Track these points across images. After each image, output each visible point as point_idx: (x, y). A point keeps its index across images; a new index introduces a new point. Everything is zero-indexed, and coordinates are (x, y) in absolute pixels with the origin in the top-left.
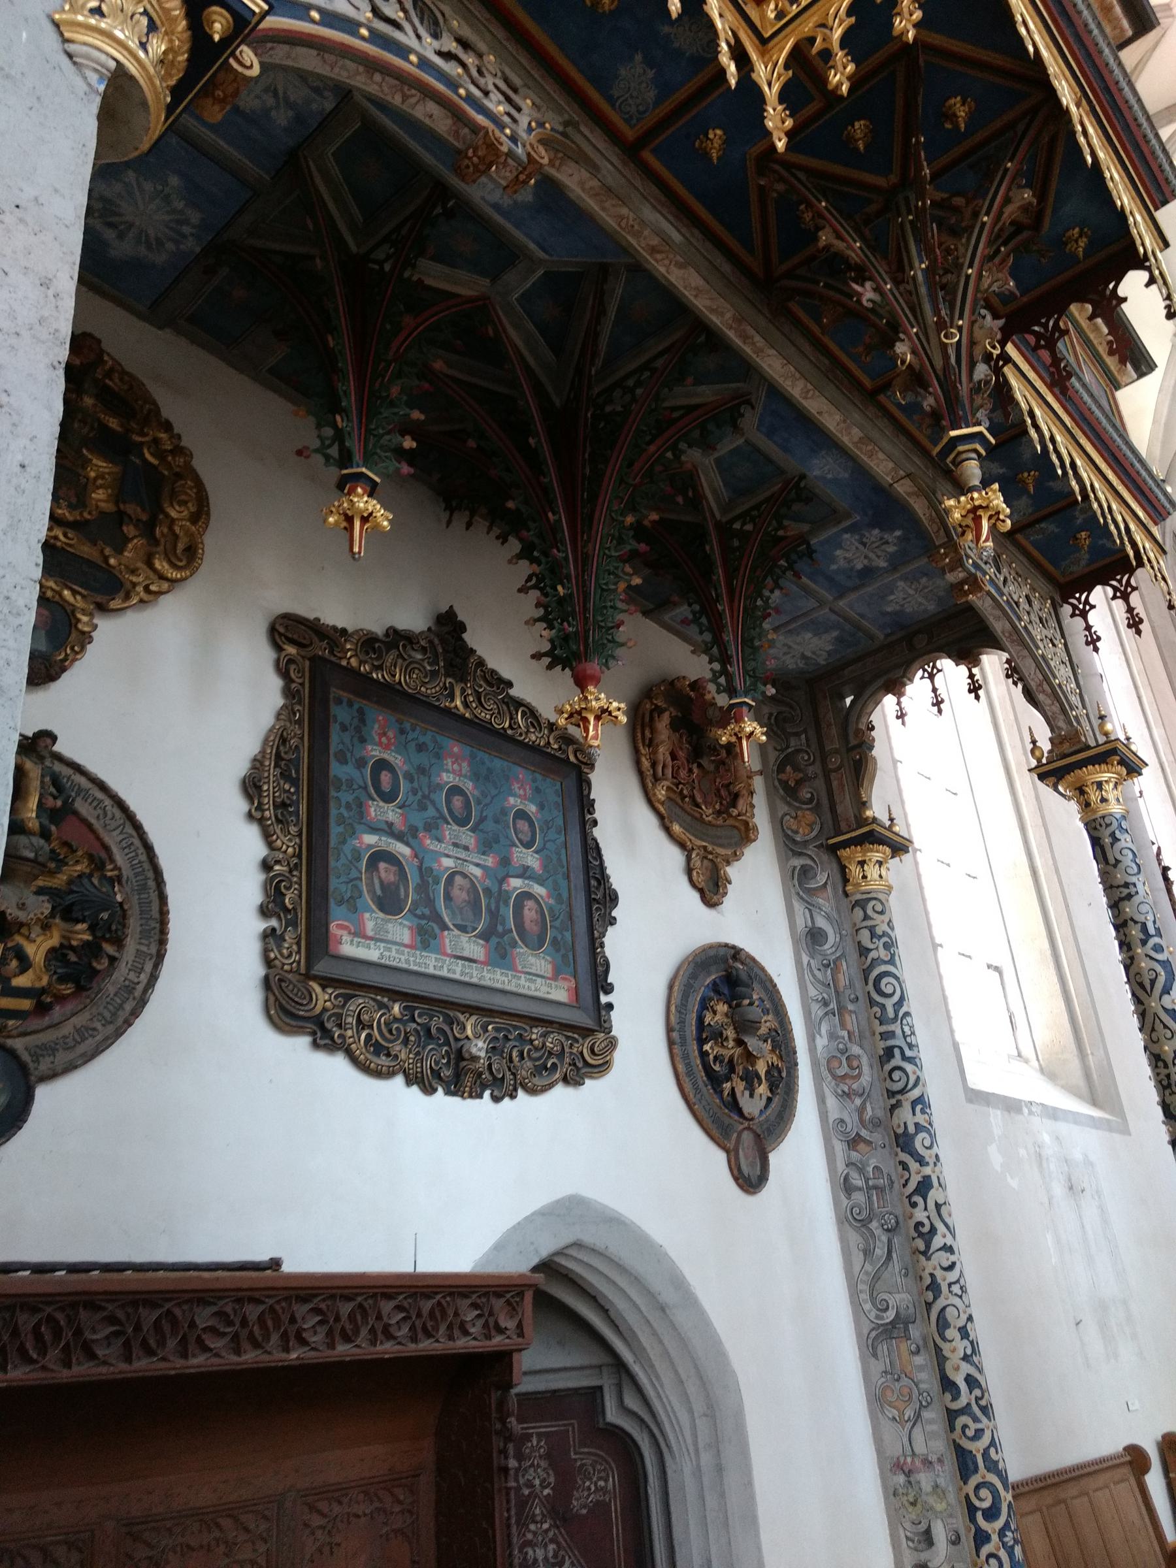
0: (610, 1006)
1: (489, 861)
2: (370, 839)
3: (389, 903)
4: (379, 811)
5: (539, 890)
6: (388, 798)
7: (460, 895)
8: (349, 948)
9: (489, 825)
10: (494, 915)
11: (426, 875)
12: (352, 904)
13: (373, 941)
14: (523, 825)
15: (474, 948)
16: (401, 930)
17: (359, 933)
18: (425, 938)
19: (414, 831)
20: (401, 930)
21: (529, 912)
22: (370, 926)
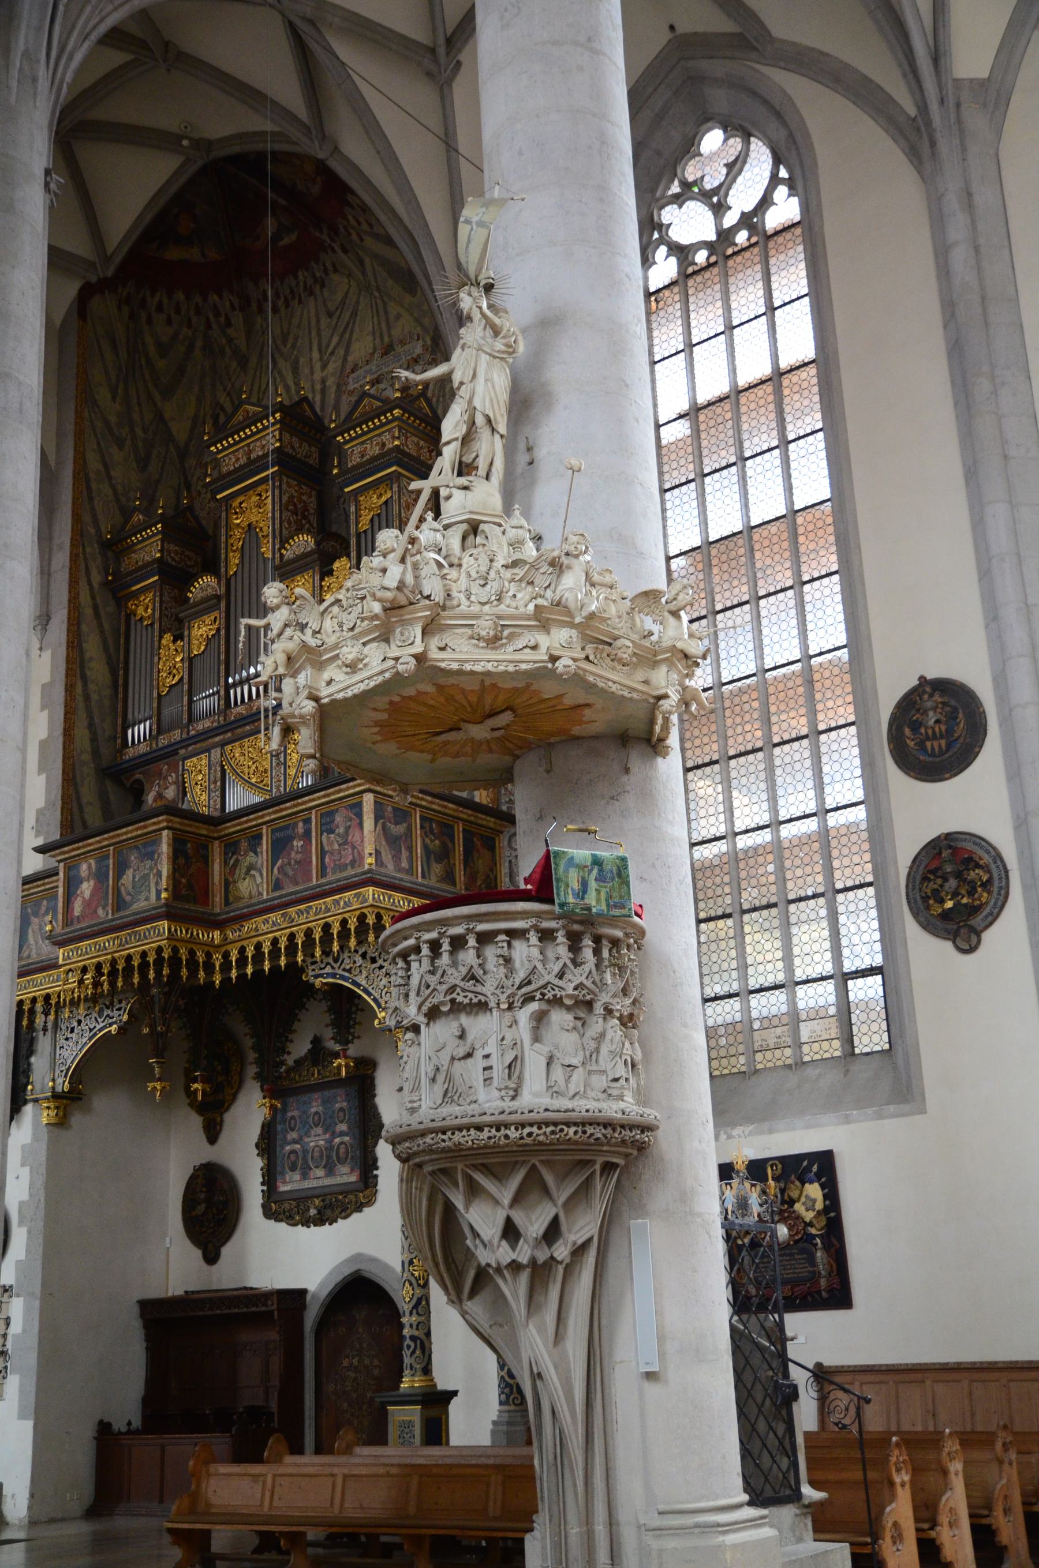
0: (376, 1176)
1: (327, 1136)
2: (288, 1148)
3: (293, 1169)
4: (293, 1135)
5: (347, 1139)
6: (292, 1130)
7: (316, 1154)
8: (283, 1188)
9: (328, 1121)
10: (329, 1157)
11: (305, 1152)
12: (283, 1174)
13: (290, 1183)
14: (341, 1114)
15: (320, 1172)
16: (297, 1176)
17: (284, 1182)
18: (305, 1176)
19: (301, 1138)
20: (297, 1176)
21: (342, 1150)
22: (288, 1179)
